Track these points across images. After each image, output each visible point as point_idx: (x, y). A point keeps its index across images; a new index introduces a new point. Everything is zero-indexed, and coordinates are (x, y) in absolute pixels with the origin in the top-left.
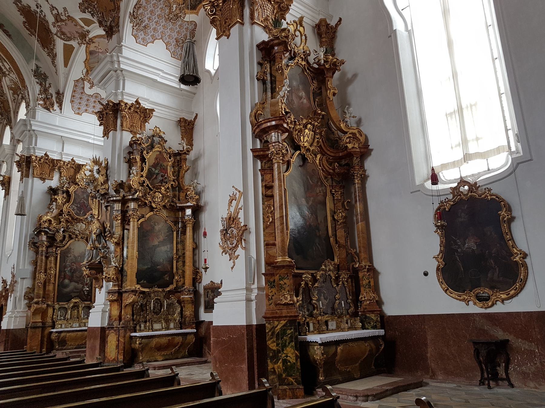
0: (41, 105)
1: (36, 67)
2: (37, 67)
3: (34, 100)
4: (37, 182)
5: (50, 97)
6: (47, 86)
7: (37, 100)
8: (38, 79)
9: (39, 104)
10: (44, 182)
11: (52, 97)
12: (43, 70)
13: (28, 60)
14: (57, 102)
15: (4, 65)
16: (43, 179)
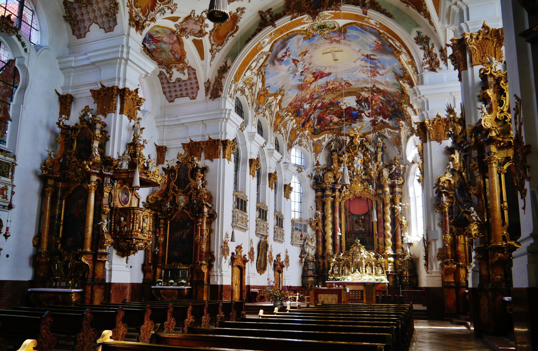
0: (427, 68)
1: (417, 34)
2: (419, 33)
3: (421, 65)
4: (434, 144)
5: (435, 57)
6: (430, 48)
7: (423, 65)
8: (421, 45)
9: (425, 69)
10: (441, 144)
11: (436, 56)
12: (424, 34)
13: (409, 31)
14: (442, 60)
15: (396, 45)
16: (439, 141)
